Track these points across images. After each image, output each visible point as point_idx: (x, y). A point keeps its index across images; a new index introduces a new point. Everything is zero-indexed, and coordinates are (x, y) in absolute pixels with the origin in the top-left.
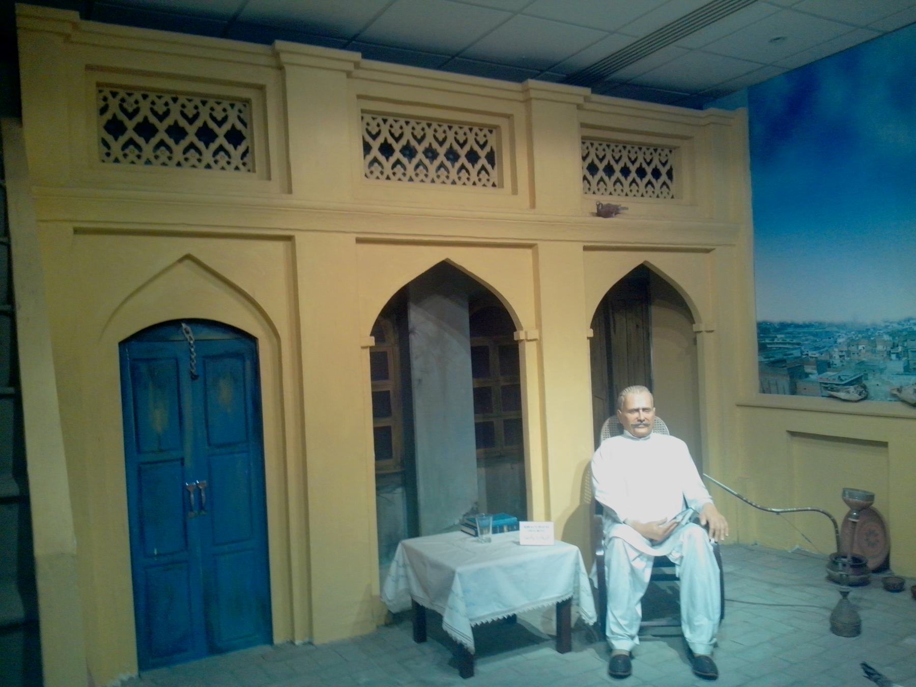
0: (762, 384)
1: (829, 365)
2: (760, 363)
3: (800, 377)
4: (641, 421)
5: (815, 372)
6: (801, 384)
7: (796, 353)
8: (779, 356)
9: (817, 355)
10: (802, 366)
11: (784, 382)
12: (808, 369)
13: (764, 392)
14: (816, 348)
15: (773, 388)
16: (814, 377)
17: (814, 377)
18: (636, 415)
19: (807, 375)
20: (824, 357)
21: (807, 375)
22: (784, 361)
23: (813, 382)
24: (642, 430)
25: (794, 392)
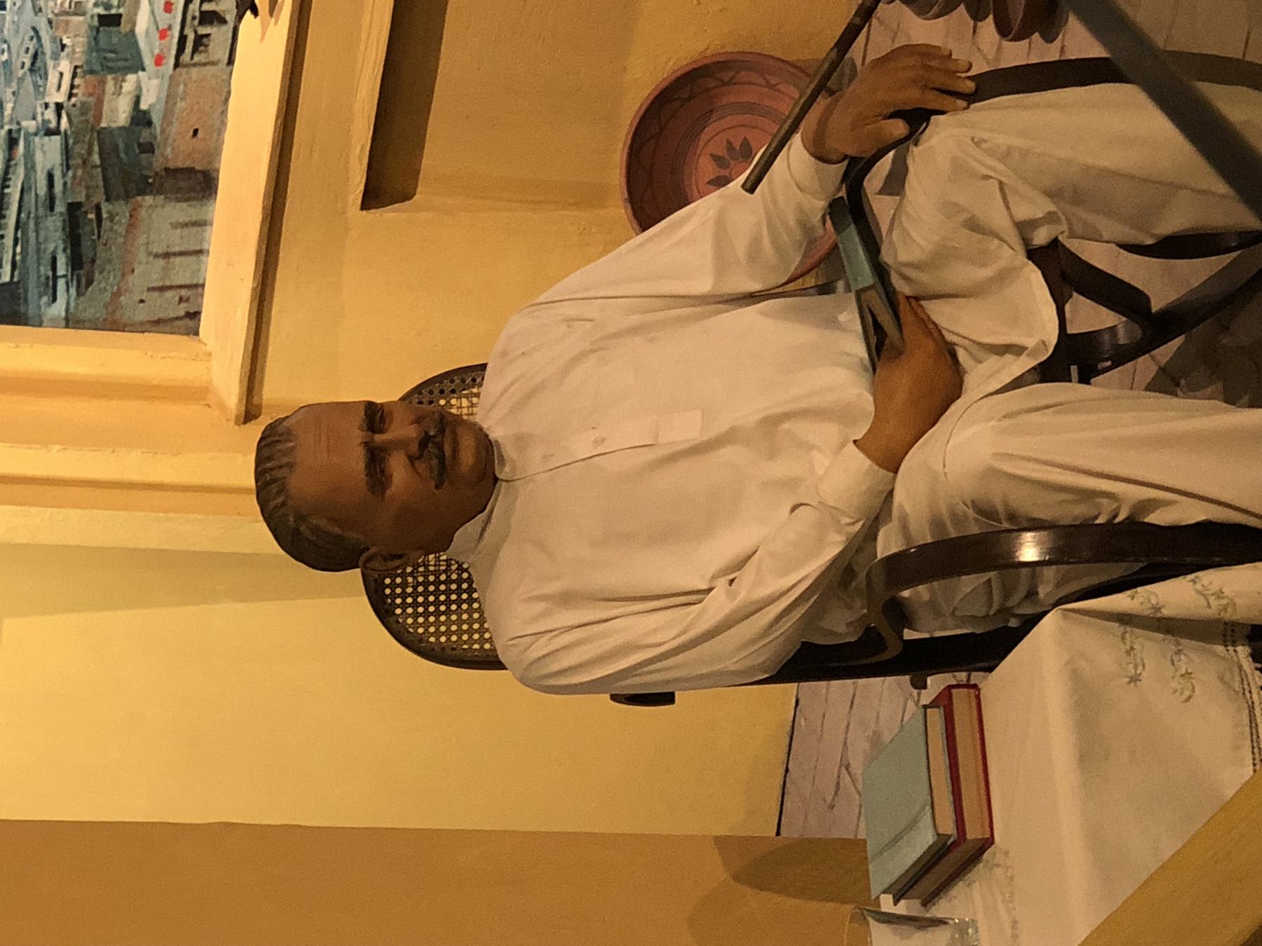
0: (158, 324)
1: (110, 21)
2: (71, 321)
3: (149, 148)
4: (425, 441)
5: (131, 78)
6: (175, 150)
7: (49, 153)
8: (54, 226)
9: (65, 66)
10: (104, 136)
11: (161, 217)
12: (118, 113)
13: (195, 315)
14: (37, 66)
15: (181, 272)
16: (150, 87)
17: (150, 87)
18: (398, 468)
19: (141, 118)
20: (76, 39)
21: (141, 118)
22: (73, 208)
23: (170, 98)
24: (467, 457)
25: (200, 183)
